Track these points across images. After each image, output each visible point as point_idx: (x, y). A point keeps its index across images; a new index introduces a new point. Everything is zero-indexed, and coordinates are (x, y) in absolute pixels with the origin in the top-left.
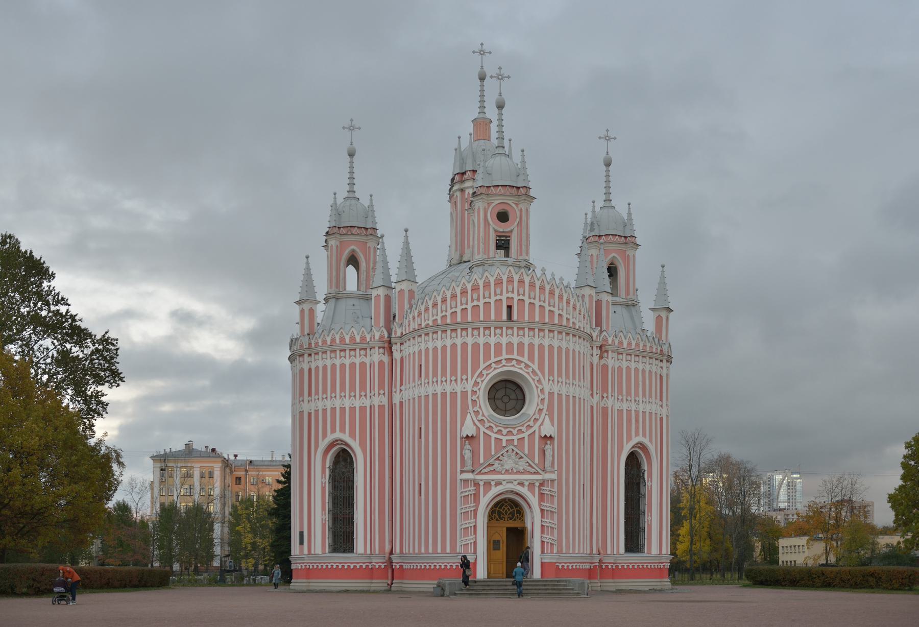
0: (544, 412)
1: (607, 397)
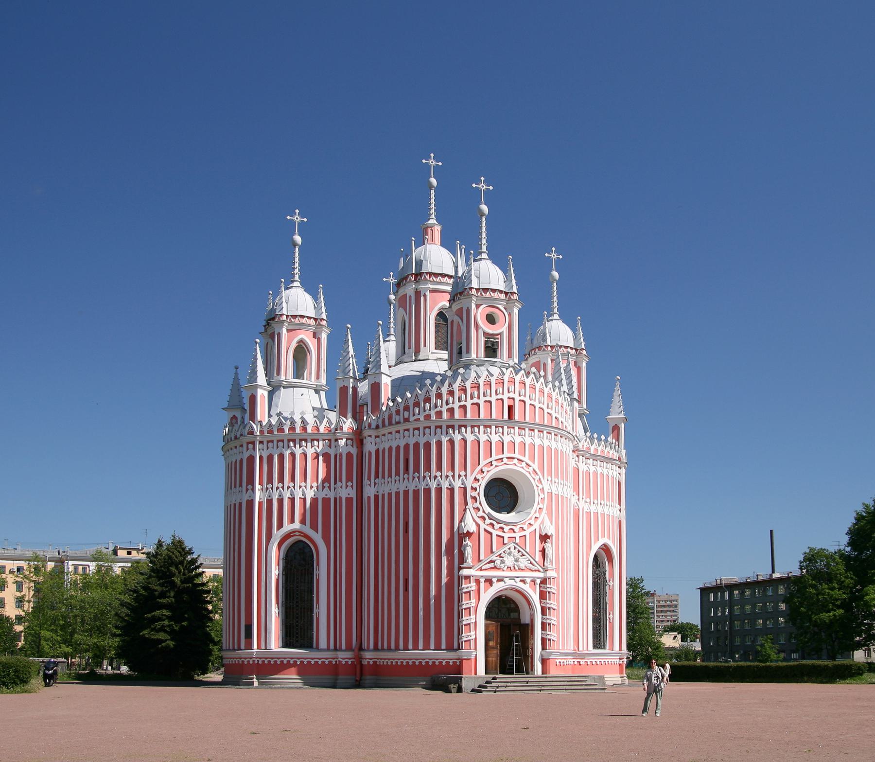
0: (544, 511)
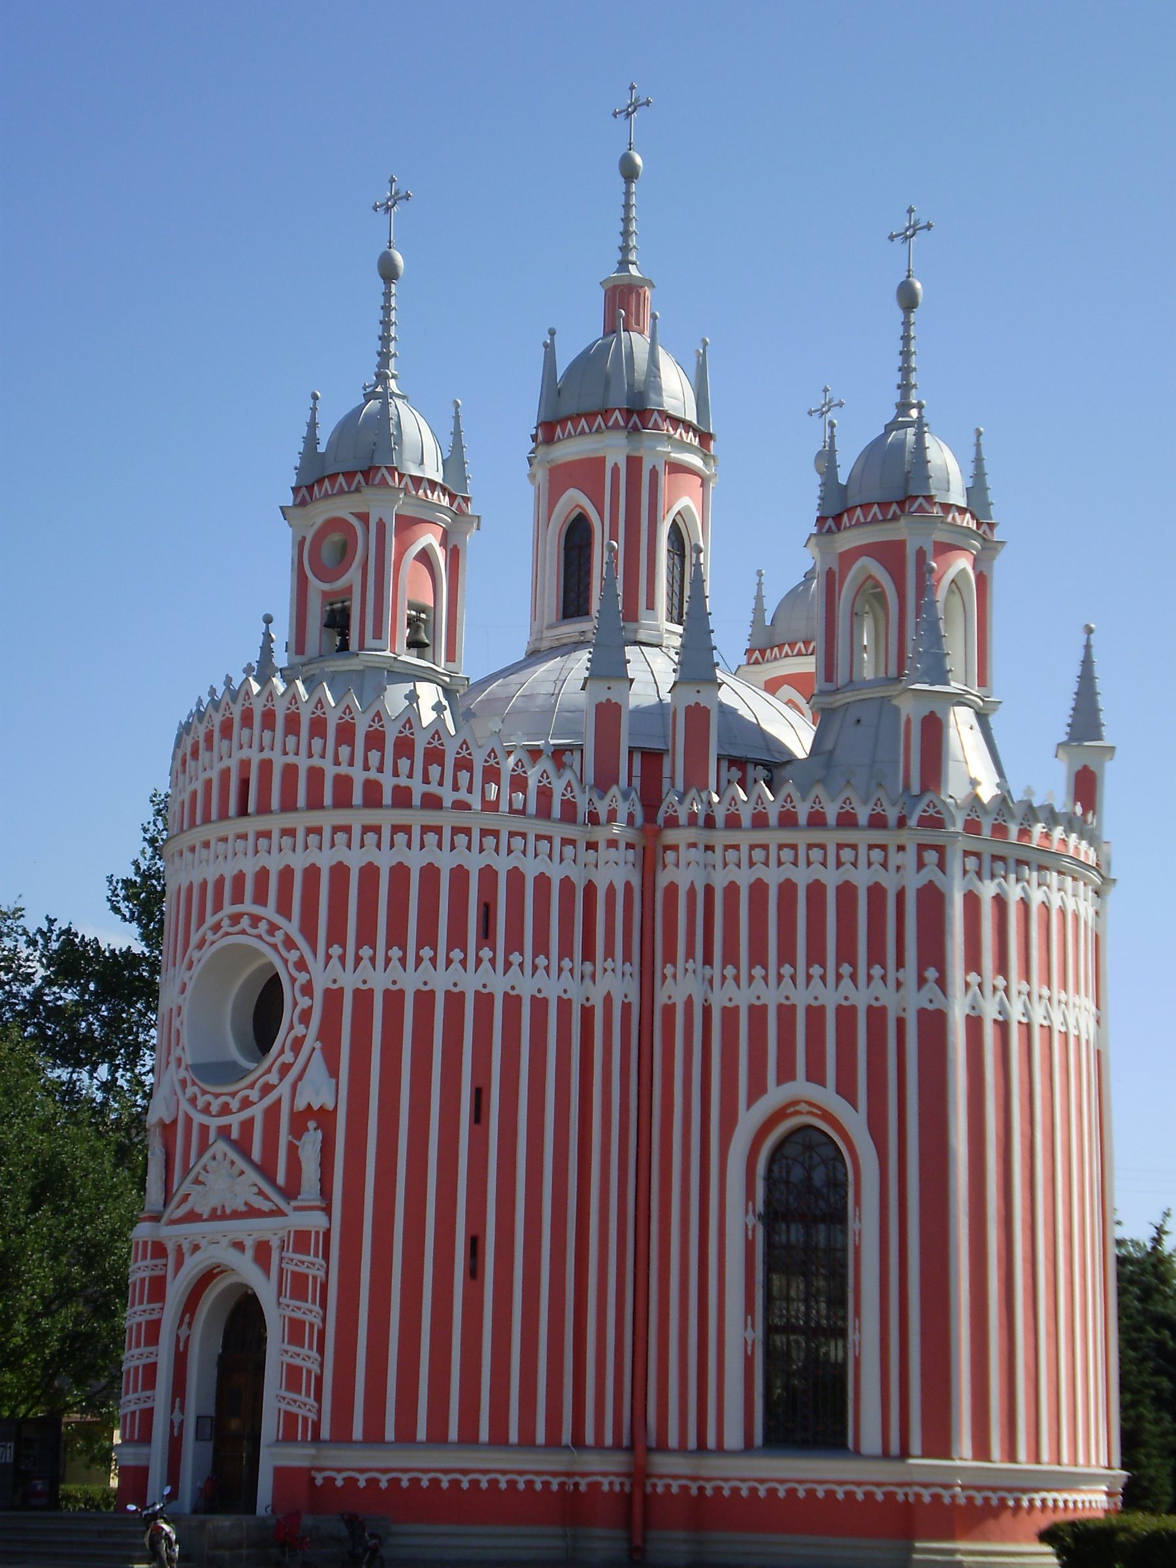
1: (674, 976)
